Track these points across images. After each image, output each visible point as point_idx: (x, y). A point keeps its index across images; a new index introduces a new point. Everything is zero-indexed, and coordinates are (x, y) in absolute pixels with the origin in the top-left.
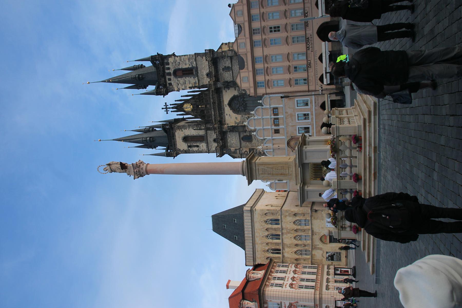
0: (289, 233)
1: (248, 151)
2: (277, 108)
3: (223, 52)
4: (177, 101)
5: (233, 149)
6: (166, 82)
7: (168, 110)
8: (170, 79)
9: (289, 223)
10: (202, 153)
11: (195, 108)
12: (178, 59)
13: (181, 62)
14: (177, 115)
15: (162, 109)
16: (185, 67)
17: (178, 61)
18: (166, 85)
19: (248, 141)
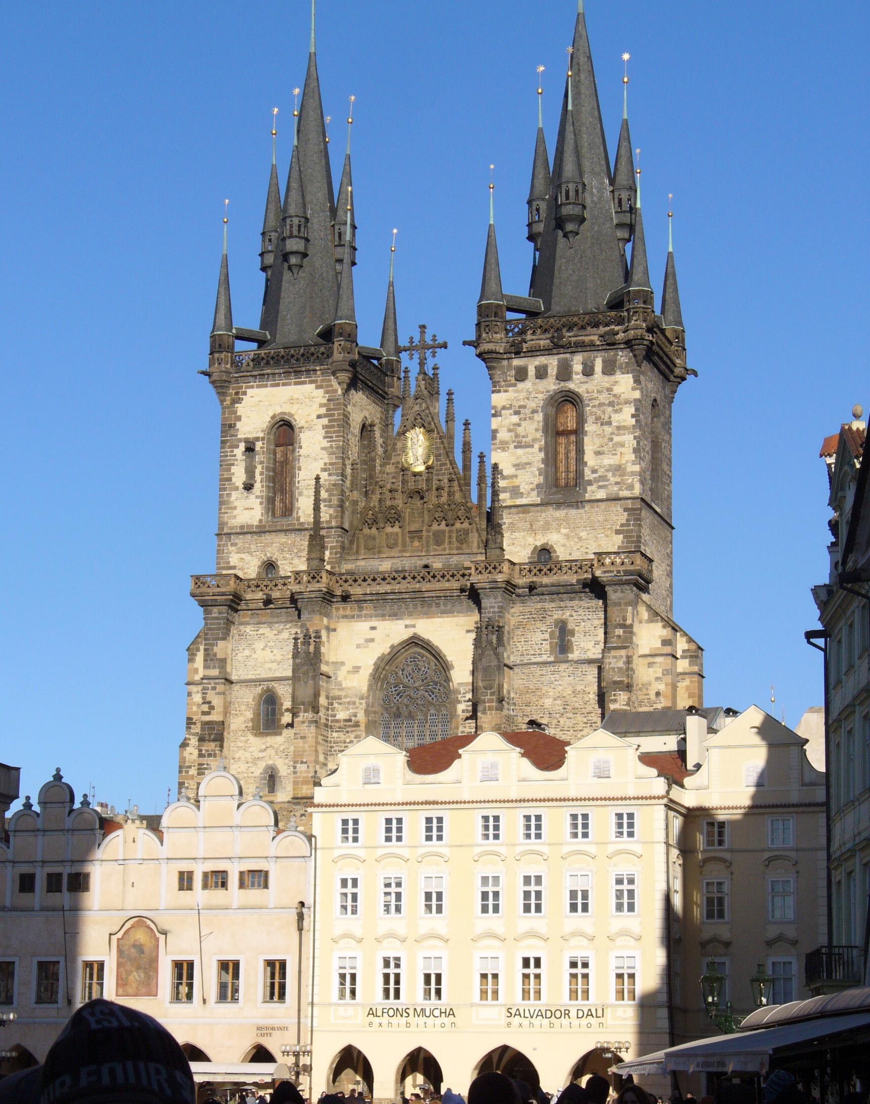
1: (215, 717)
2: (266, 886)
3: (628, 629)
4: (450, 400)
5: (221, 648)
6: (534, 352)
7: (416, 356)
8: (541, 373)
10: (221, 503)
11: (411, 485)
12: (626, 417)
13: (608, 429)
15: (423, 327)
16: (590, 446)
17: (617, 419)
19: (257, 715)
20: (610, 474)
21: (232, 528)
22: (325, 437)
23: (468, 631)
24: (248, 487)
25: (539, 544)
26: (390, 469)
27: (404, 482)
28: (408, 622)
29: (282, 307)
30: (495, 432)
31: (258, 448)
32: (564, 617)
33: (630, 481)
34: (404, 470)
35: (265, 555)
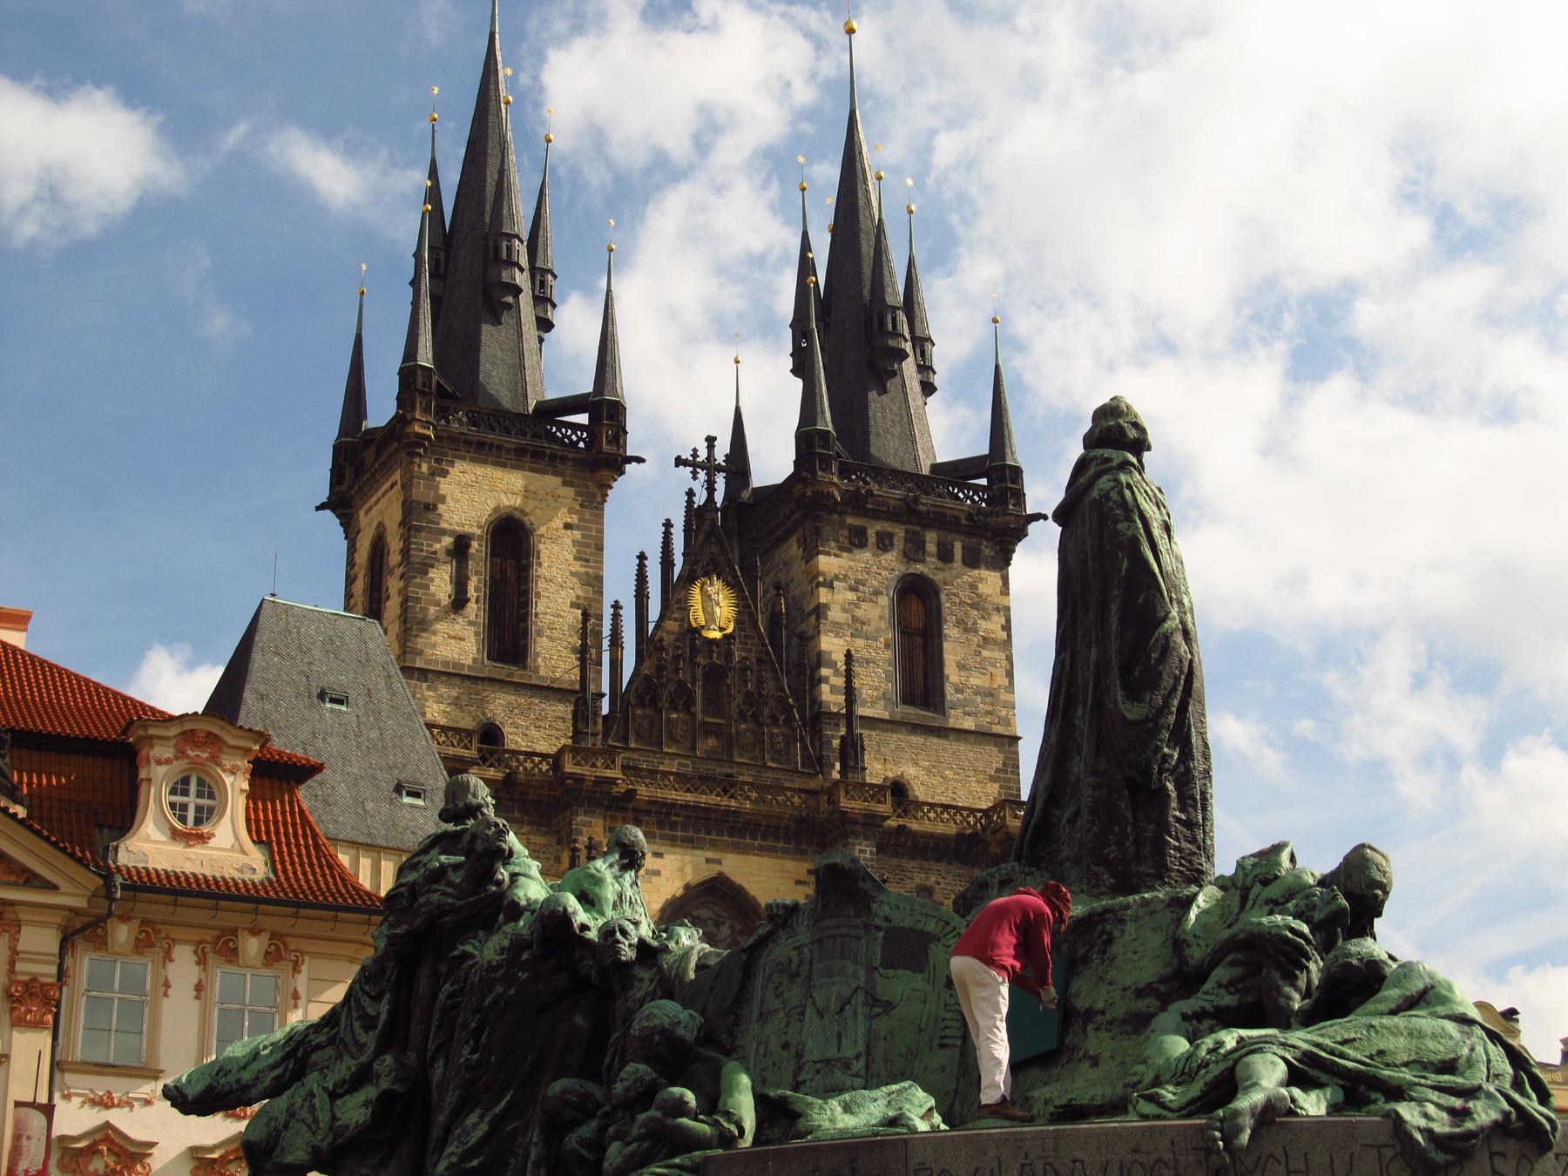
6: (876, 515)
8: (884, 542)
14: (668, 525)
15: (711, 440)
16: (952, 653)
20: (979, 699)
21: (429, 662)
22: (576, 559)
23: (798, 882)
24: (459, 603)
25: (890, 775)
26: (671, 625)
27: (694, 651)
28: (710, 854)
29: (482, 356)
30: (827, 606)
31: (472, 551)
32: (928, 883)
33: (1004, 713)
34: (695, 632)
35: (484, 714)
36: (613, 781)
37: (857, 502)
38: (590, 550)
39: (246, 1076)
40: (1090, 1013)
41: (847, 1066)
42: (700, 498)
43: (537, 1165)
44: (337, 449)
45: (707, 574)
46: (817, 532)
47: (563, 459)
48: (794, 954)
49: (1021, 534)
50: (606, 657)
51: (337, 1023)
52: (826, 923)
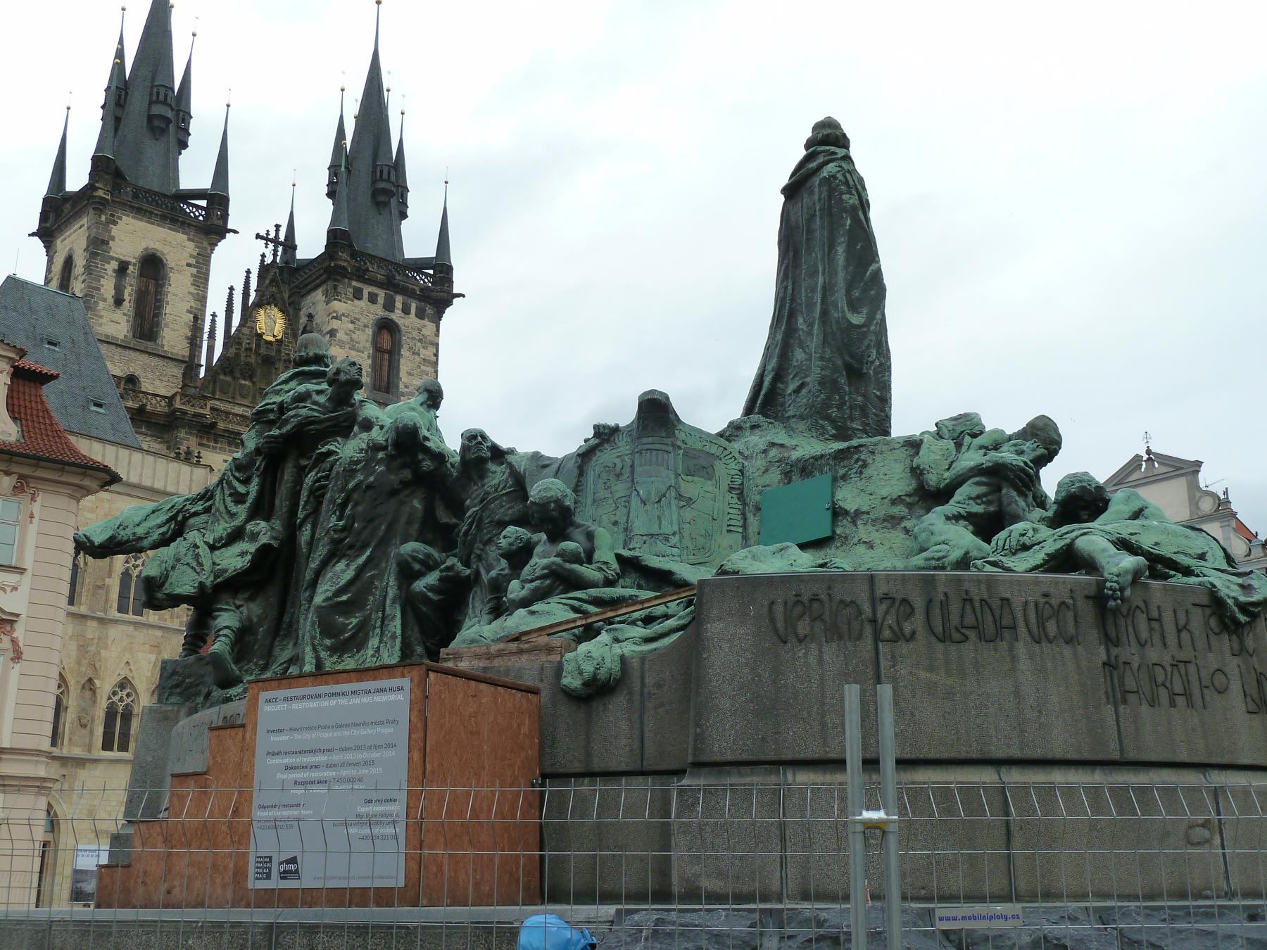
0: (83, 648)
8: (373, 299)
9: (127, 657)
11: (263, 351)
14: (248, 272)
15: (278, 227)
17: (423, 352)
18: (361, 279)
26: (246, 330)
27: (258, 346)
36: (204, 416)
37: (361, 276)
38: (202, 279)
39: (140, 531)
40: (858, 513)
41: (667, 540)
42: (269, 260)
43: (394, 602)
44: (46, 201)
45: (269, 304)
46: (335, 288)
47: (189, 225)
48: (617, 461)
49: (449, 303)
50: (205, 344)
51: (211, 497)
52: (645, 440)
